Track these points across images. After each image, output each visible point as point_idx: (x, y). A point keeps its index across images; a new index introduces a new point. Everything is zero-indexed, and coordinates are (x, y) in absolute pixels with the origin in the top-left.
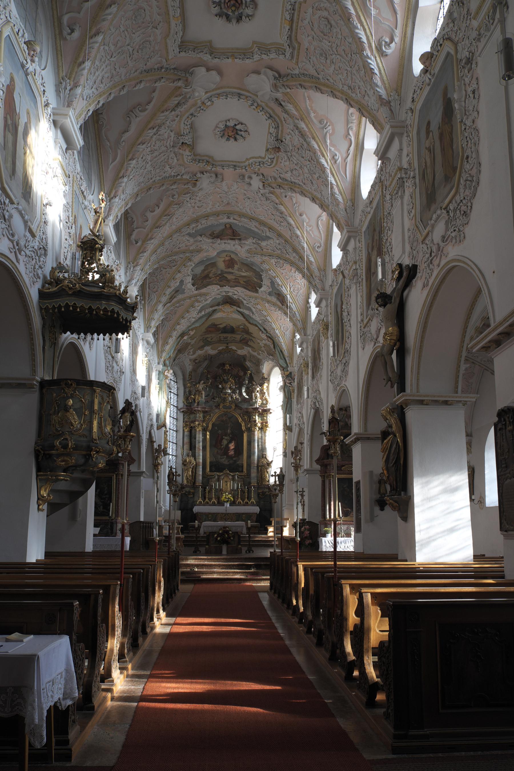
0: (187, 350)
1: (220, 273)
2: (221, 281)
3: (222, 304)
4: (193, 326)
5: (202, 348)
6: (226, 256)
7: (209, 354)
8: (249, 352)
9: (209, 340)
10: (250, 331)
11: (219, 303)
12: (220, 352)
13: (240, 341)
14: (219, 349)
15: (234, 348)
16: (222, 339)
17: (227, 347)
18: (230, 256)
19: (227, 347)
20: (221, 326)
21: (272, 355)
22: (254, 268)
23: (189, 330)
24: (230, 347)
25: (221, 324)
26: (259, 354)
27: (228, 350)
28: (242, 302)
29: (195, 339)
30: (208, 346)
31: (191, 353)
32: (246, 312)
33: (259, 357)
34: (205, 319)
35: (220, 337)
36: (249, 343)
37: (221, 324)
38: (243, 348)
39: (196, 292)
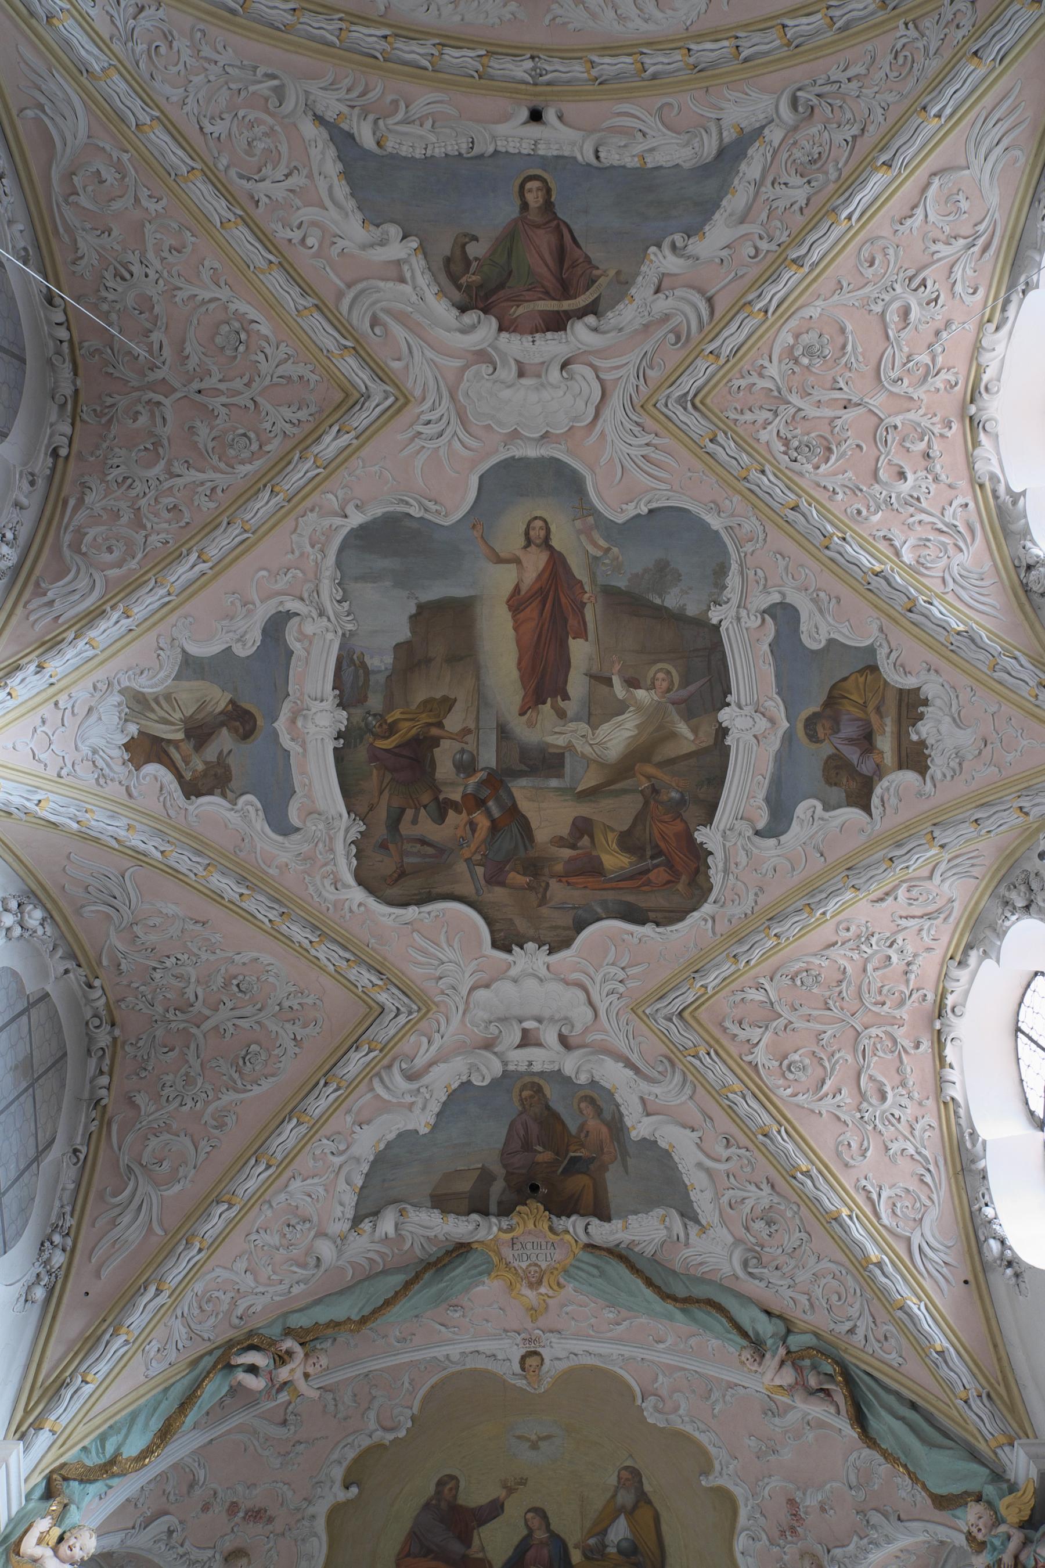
1: (488, 758)
2: (495, 879)
3: (505, 1210)
4: (322, 1315)
6: (529, 542)
11: (485, 1177)
18: (546, 543)
20: (496, 1541)
22: (672, 600)
23: (288, 1332)
25: (495, 1509)
28: (617, 1126)
32: (643, 1230)
34: (396, 1280)
37: (495, 1509)
39: (358, 895)
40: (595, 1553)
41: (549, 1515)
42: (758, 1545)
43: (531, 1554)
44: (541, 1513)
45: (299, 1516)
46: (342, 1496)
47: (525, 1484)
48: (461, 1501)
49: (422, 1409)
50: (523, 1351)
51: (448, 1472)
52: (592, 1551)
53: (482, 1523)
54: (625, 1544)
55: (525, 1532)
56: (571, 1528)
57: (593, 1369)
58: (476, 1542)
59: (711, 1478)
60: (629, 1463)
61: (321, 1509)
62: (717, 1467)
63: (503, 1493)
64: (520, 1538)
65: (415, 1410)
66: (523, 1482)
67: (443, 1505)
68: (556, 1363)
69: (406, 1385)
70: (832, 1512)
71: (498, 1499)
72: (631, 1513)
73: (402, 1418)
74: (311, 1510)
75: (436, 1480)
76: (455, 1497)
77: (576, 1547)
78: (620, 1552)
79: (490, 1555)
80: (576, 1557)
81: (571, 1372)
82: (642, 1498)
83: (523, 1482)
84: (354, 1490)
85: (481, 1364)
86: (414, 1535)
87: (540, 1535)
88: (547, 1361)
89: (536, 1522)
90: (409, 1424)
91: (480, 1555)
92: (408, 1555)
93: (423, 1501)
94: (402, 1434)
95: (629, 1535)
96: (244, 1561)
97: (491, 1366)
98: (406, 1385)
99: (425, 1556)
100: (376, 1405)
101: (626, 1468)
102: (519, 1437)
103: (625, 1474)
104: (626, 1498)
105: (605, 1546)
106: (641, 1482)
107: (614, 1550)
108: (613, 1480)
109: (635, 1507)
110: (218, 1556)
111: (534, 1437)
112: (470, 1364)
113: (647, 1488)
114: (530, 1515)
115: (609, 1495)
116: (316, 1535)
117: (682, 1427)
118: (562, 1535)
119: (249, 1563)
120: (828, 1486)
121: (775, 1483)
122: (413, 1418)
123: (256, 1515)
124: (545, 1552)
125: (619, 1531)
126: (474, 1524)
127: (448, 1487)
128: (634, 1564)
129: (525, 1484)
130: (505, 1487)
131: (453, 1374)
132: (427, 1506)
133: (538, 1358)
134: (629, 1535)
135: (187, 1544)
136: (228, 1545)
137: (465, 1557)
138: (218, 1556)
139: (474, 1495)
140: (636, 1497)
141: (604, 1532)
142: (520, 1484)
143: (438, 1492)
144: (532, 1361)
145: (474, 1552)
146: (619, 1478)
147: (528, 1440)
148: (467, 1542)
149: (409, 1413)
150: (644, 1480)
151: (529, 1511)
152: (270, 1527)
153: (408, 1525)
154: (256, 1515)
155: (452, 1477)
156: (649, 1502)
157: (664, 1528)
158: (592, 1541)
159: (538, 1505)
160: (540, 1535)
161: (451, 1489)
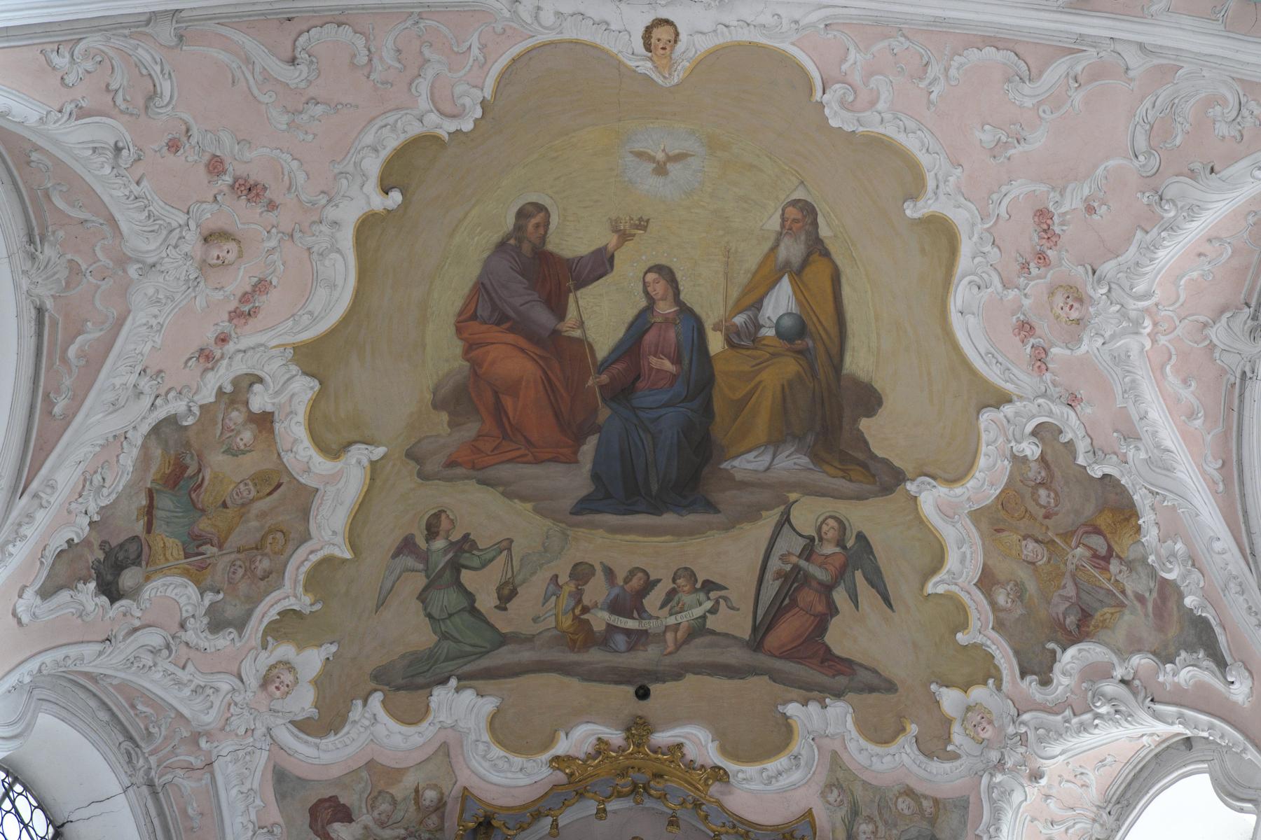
0: (268, 610)
5: (408, 682)
7: (466, 795)
8: (839, 779)
9: (482, 585)
10: (858, 362)
12: (575, 782)
13: (757, 641)
14: (562, 747)
15: (700, 743)
16: (600, 619)
17: (638, 729)
19: (638, 729)
20: (601, 316)
21: (1081, 627)
24: (663, 738)
25: (601, 264)
26: (936, 744)
27: (636, 773)
29: (360, 455)
30: (466, 679)
31: (304, 702)
33: (941, 777)
35: (581, 573)
36: (840, 638)
37: (601, 264)
38: (784, 734)
40: (743, 339)
41: (679, 276)
42: (986, 293)
43: (650, 338)
44: (667, 273)
45: (316, 218)
46: (379, 202)
47: (645, 228)
48: (550, 247)
49: (496, 92)
50: (648, 19)
51: (534, 198)
52: (738, 334)
53: (582, 283)
54: (787, 322)
55: (643, 303)
56: (710, 299)
57: (752, 46)
58: (572, 313)
59: (920, 203)
60: (799, 195)
61: (349, 214)
62: (931, 184)
63: (613, 240)
64: (636, 311)
65: (488, 93)
66: (643, 225)
67: (526, 248)
68: (697, 38)
69: (475, 51)
70: (1104, 208)
71: (605, 247)
72: (798, 273)
73: (467, 101)
74: (331, 213)
75: (515, 209)
76: (543, 239)
77: (716, 328)
78: (779, 334)
79: (592, 335)
80: (716, 344)
81: (716, 53)
82: (817, 248)
83: (643, 225)
84: (396, 197)
85: (586, 34)
86: (481, 288)
87: (665, 308)
88: (683, 36)
89: (659, 288)
90: (478, 113)
91: (577, 333)
92: (474, 317)
93: (496, 238)
94: (467, 126)
95: (794, 308)
96: (232, 246)
97: (600, 39)
98: (475, 51)
99: (498, 324)
100: (430, 73)
101: (795, 203)
102: (640, 155)
103: (793, 213)
104: (792, 250)
105: (758, 327)
106: (815, 224)
107: (771, 332)
108: (775, 224)
109: (805, 263)
110: (192, 225)
111: (660, 156)
112: (570, 33)
113: (824, 232)
114: (651, 277)
115: (767, 246)
116: (339, 251)
117: (881, 130)
118: (697, 310)
119: (240, 255)
120: (1100, 171)
121: (1019, 188)
122: (484, 104)
123: (249, 189)
124: (672, 334)
125: (780, 303)
126: (570, 284)
127: (534, 221)
128: (800, 352)
129: (645, 228)
130: (616, 230)
131: (544, 45)
132: (502, 246)
133: (671, 29)
134: (794, 308)
135: (145, 183)
136: (209, 216)
137: (556, 333)
138: (192, 225)
139: (573, 239)
140: (808, 251)
141: (758, 305)
142: (638, 227)
143: (519, 228)
144: (662, 33)
145: (568, 327)
146: (783, 219)
147: (652, 159)
148: (560, 313)
149: (478, 95)
150: (820, 220)
151: (650, 270)
152: (271, 217)
153: (471, 271)
154: (249, 189)
155: (540, 208)
156: (826, 254)
157: (846, 291)
158: (739, 320)
159: (663, 261)
160: (665, 308)
161: (537, 226)
